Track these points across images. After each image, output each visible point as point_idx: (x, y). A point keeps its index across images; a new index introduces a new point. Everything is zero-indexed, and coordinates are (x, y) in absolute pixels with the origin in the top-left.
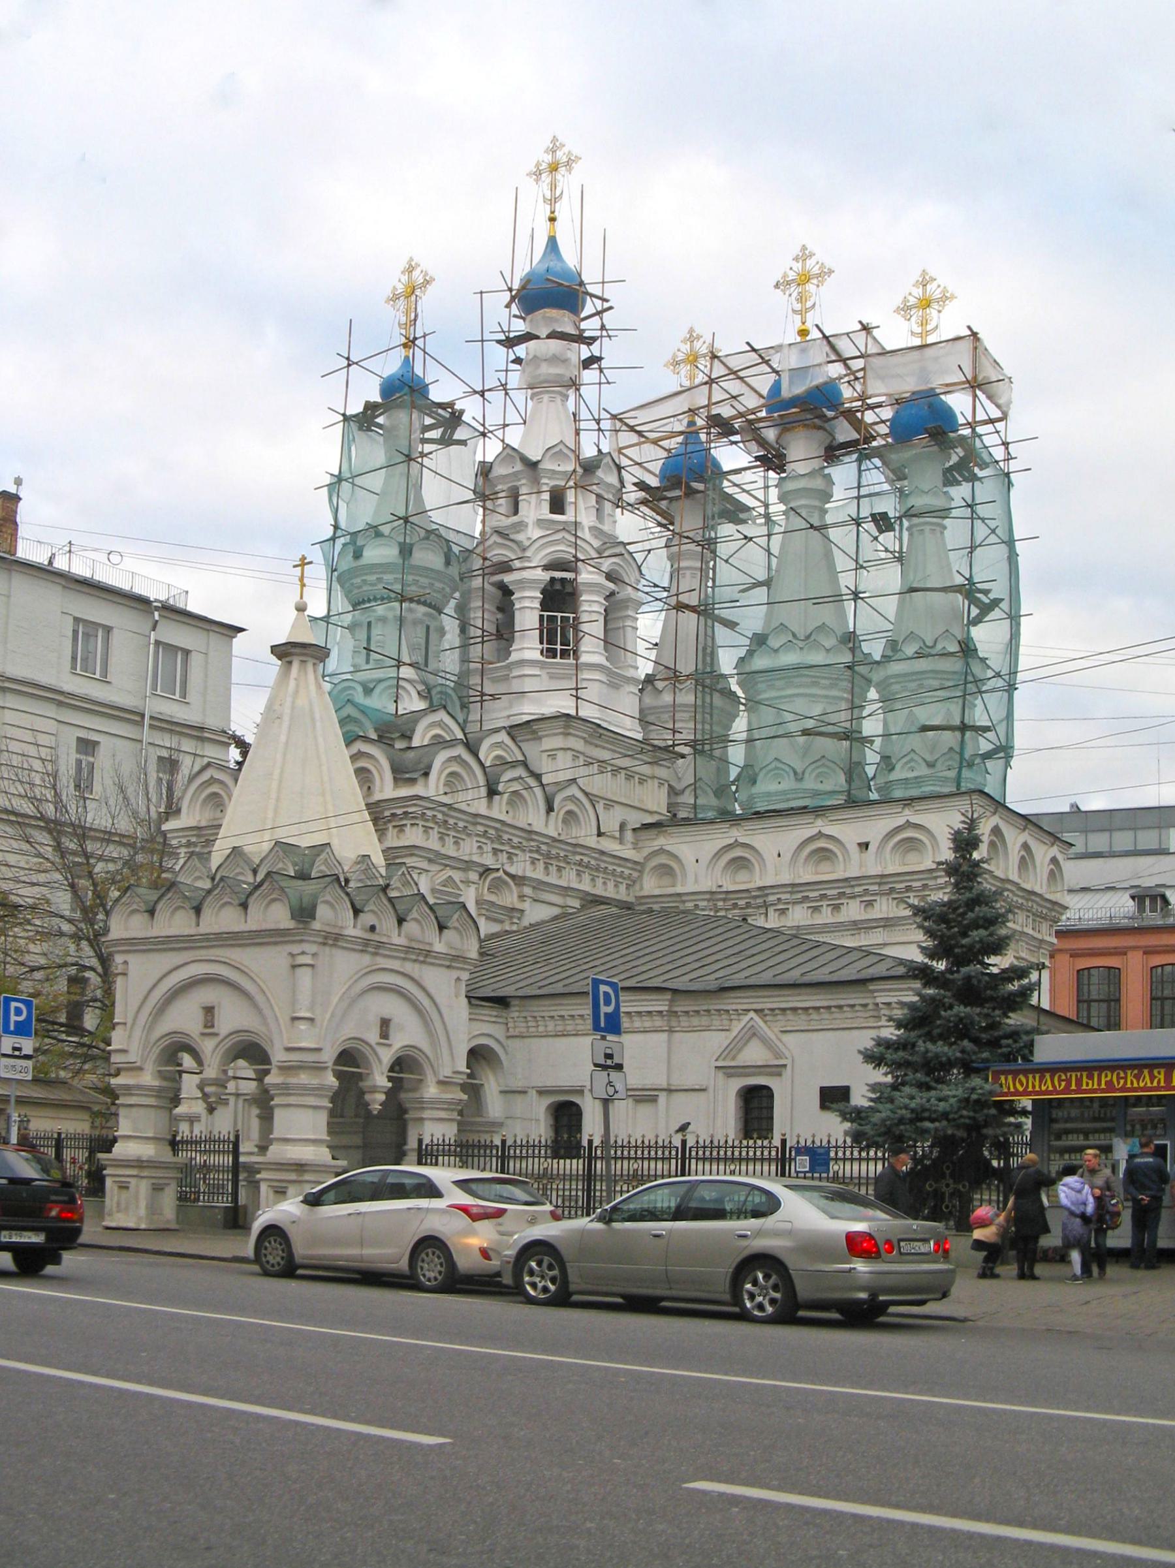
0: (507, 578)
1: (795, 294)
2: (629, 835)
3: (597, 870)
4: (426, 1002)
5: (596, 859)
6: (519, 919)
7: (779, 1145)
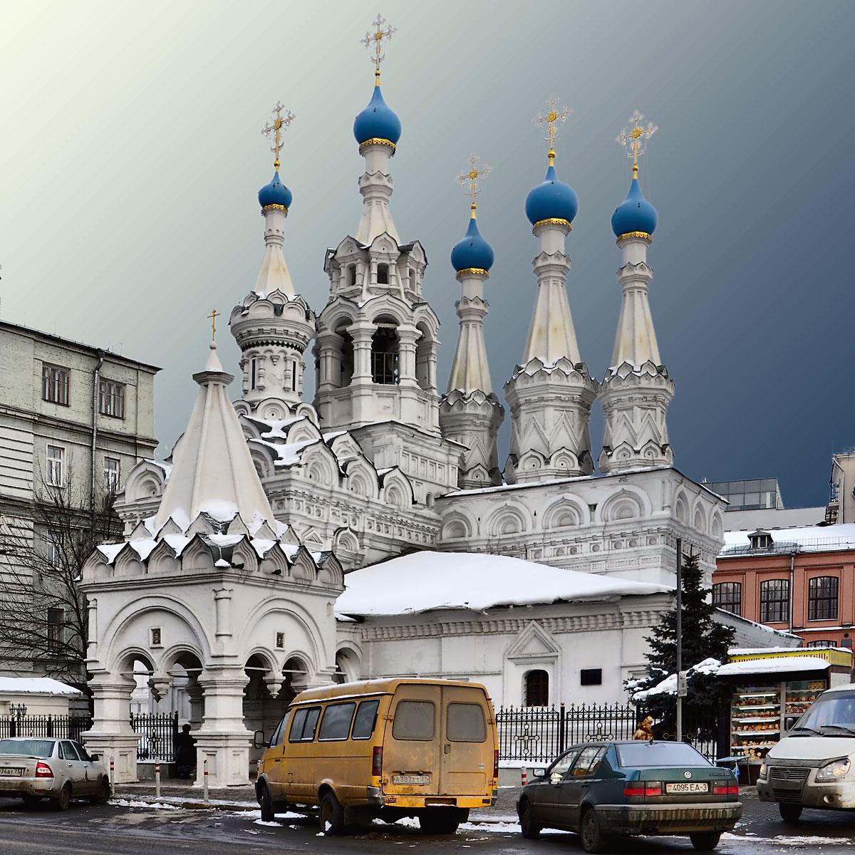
0: (349, 329)
2: (432, 502)
3: (412, 527)
4: (308, 620)
5: (411, 519)
6: (360, 561)
7: (559, 711)
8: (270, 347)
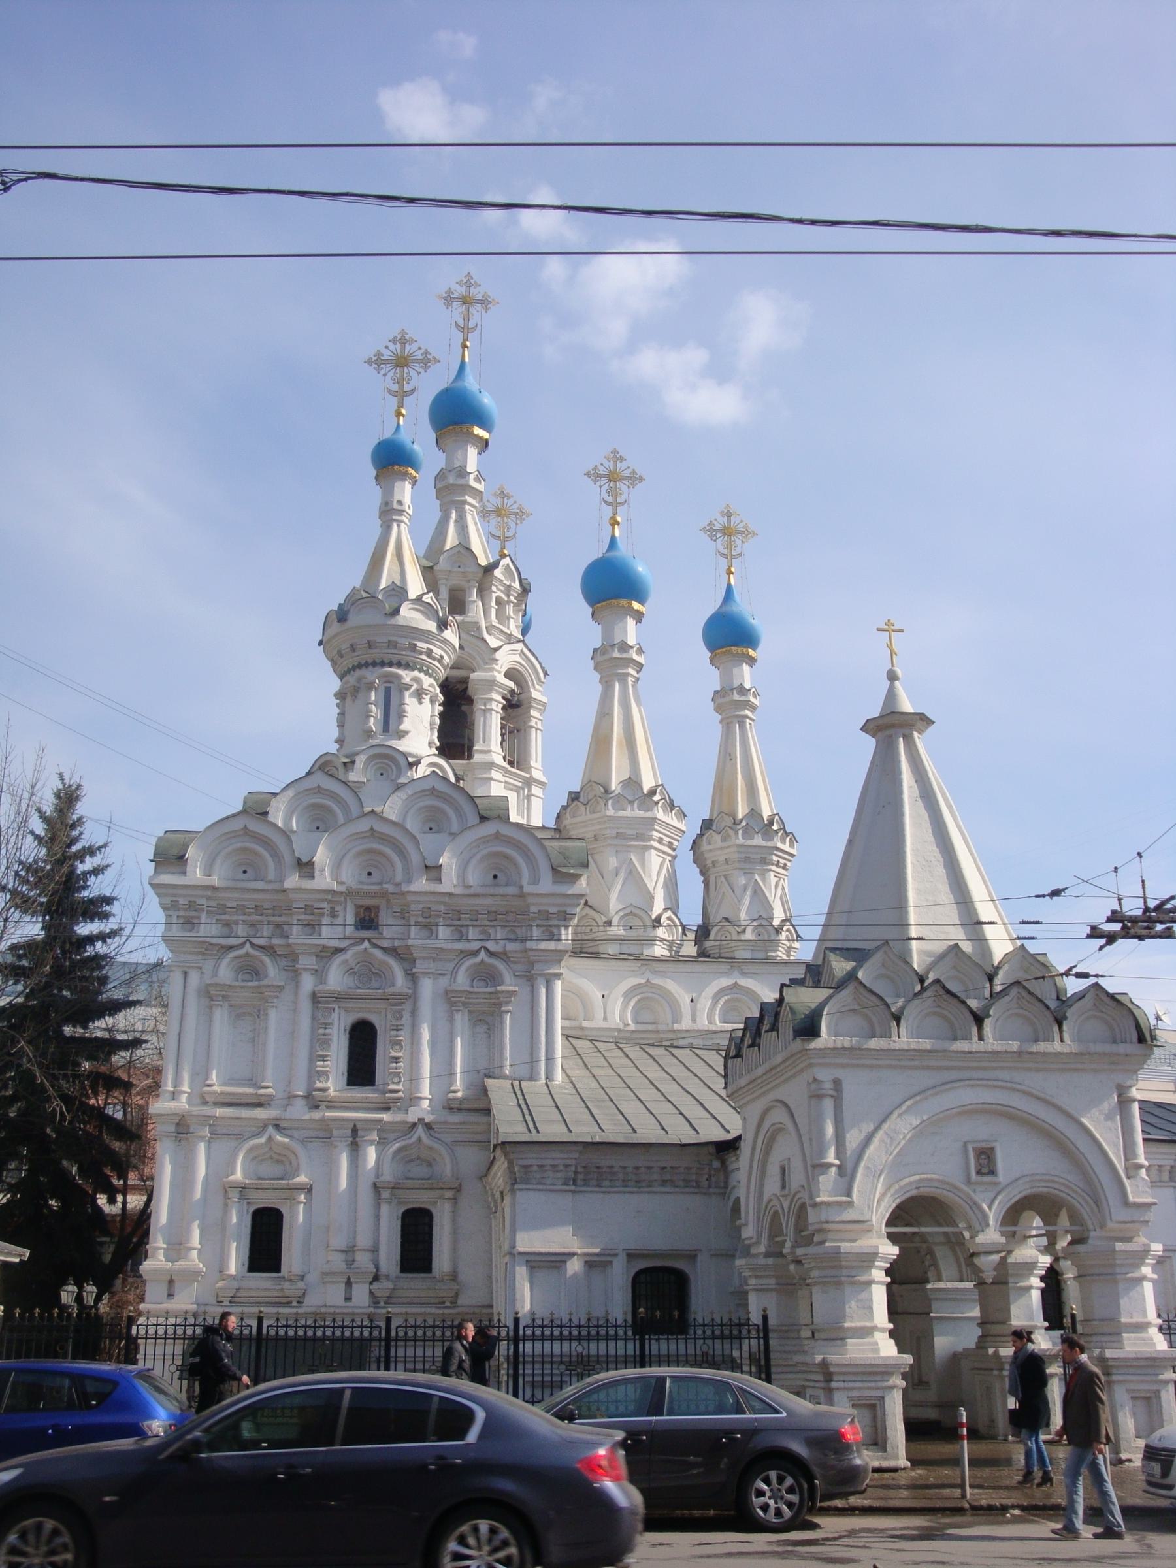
1: (605, 487)
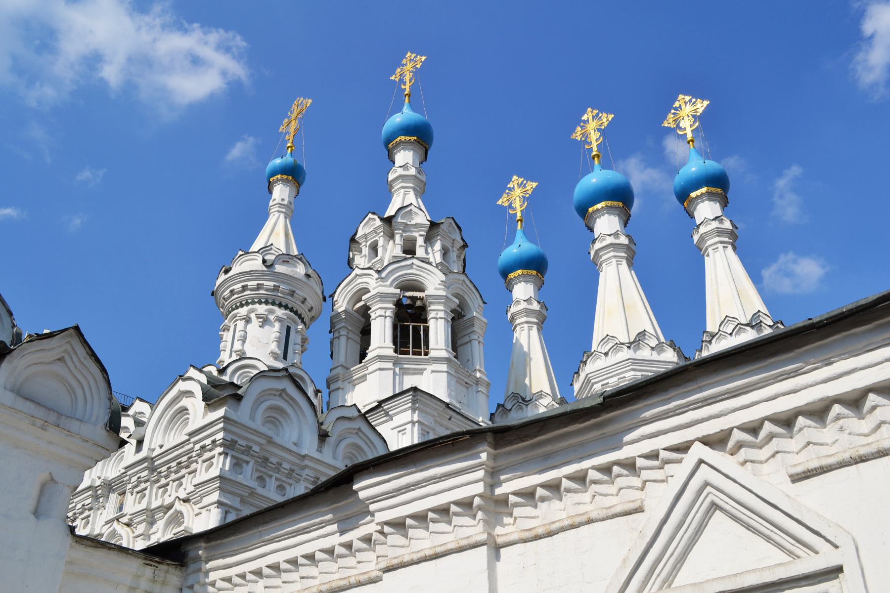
8: (257, 306)
